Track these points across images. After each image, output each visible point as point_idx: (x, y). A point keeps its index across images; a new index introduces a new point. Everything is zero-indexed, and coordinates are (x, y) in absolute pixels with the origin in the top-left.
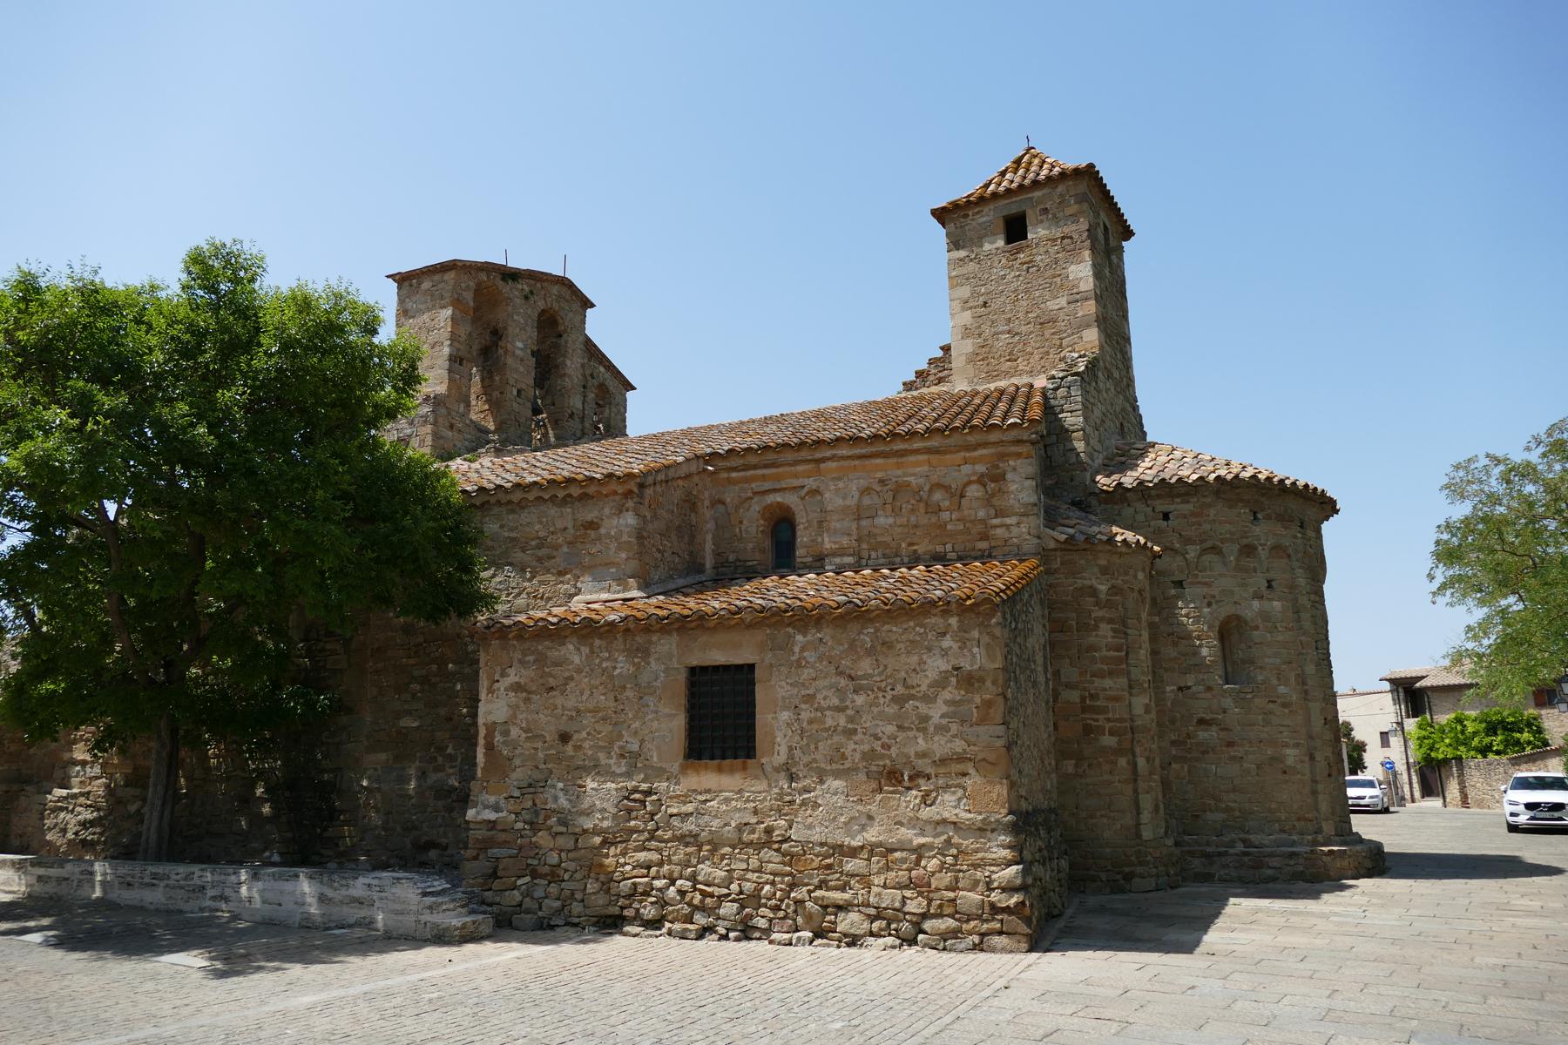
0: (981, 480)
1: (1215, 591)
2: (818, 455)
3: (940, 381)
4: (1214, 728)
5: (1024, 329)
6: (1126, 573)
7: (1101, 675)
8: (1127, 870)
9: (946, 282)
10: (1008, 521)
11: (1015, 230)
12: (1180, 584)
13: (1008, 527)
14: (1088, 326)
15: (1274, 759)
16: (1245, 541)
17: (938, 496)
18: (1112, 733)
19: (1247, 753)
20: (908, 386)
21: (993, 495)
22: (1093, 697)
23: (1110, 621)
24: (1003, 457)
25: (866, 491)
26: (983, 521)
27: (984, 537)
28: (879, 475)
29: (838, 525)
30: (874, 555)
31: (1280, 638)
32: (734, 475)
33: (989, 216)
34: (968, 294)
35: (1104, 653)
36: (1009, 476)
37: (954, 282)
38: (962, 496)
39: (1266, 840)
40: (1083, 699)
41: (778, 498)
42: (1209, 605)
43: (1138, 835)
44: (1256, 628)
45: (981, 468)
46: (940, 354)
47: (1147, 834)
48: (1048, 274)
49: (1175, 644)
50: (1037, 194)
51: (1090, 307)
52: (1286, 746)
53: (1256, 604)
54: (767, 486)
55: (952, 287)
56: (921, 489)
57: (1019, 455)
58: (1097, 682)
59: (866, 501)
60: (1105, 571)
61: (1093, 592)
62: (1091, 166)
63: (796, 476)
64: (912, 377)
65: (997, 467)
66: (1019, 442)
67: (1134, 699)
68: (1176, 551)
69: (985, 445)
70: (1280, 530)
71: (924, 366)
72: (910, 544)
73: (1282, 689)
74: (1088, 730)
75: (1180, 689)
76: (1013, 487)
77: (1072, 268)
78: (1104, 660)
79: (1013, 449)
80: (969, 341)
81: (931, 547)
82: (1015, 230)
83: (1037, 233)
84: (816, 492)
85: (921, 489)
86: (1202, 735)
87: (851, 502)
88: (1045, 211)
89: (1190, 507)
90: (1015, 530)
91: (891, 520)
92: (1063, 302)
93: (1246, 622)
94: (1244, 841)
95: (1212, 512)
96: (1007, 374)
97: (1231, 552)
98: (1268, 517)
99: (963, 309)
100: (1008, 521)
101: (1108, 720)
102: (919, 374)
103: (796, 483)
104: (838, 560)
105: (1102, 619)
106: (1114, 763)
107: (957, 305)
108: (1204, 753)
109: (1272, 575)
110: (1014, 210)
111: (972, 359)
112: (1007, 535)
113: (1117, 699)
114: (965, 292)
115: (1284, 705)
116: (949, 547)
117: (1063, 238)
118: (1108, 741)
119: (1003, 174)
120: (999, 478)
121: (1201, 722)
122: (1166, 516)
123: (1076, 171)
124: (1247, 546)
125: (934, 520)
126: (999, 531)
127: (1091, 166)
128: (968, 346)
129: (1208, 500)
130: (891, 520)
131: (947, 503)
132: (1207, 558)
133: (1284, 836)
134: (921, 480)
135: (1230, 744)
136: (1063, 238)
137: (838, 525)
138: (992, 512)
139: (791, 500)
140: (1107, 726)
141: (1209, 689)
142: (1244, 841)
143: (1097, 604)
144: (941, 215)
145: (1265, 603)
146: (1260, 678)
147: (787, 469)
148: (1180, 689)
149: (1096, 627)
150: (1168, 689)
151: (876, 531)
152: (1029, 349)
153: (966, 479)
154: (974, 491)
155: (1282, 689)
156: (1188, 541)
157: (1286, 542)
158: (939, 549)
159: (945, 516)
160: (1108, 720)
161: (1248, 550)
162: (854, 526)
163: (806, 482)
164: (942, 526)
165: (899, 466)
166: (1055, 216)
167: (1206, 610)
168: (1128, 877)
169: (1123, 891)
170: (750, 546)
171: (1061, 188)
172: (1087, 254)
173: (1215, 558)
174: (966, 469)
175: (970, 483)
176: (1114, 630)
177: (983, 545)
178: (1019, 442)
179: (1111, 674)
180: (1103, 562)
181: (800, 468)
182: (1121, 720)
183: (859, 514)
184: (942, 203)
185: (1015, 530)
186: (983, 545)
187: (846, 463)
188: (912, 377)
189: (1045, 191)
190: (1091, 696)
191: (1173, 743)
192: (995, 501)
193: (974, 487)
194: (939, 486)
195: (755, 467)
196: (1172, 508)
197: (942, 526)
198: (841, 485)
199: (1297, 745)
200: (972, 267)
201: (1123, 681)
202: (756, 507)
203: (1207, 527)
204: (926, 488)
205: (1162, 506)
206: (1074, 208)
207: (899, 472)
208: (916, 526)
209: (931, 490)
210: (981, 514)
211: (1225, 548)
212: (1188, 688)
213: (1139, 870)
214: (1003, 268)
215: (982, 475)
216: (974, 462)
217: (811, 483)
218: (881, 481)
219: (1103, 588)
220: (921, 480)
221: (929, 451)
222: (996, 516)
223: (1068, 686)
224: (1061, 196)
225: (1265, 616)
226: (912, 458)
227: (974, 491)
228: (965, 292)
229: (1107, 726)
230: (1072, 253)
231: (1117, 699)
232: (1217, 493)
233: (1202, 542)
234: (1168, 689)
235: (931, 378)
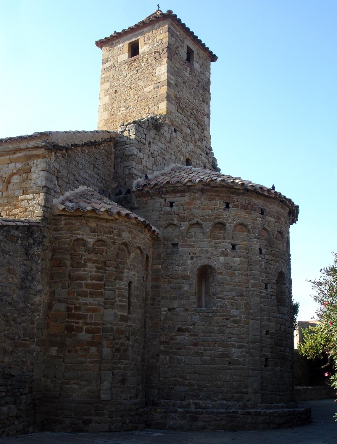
0: (18, 172)
1: (197, 250)
4: (187, 334)
6: (110, 233)
7: (84, 294)
8: (86, 418)
12: (175, 245)
14: (162, 101)
15: (224, 355)
16: (217, 220)
18: (87, 331)
19: (205, 350)
21: (23, 181)
22: (77, 308)
23: (95, 262)
24: (30, 158)
31: (237, 279)
33: (124, 46)
34: (109, 87)
35: (89, 282)
36: (32, 170)
37: (104, 80)
38: (9, 182)
39: (210, 403)
40: (69, 309)
42: (192, 258)
43: (99, 397)
44: (221, 274)
45: (19, 165)
47: (103, 397)
49: (169, 282)
51: (164, 90)
52: (234, 346)
53: (222, 259)
57: (38, 156)
58: (82, 300)
60: (93, 230)
61: (84, 243)
62: (170, 12)
65: (28, 164)
66: (37, 148)
67: (105, 310)
68: (175, 225)
69: (20, 150)
70: (243, 214)
73: (234, 311)
74: (70, 328)
75: (170, 310)
78: (87, 286)
79: (35, 152)
80: (106, 113)
86: (179, 338)
89: (186, 199)
90: (31, 203)
93: (214, 269)
94: (196, 404)
95: (198, 202)
97: (208, 226)
98: (236, 207)
101: (86, 324)
105: (89, 260)
106: (87, 350)
108: (179, 349)
109: (235, 242)
110: (134, 40)
112: (27, 205)
113: (95, 311)
114: (107, 85)
115: (234, 322)
117: (155, 52)
118: (84, 336)
120: (28, 171)
121: (180, 330)
122: (172, 205)
124: (220, 223)
126: (23, 202)
129: (197, 195)
132: (193, 230)
133: (224, 402)
135: (195, 345)
140: (85, 327)
141: (186, 310)
142: (196, 404)
143: (87, 250)
144: (101, 44)
145: (229, 258)
146: (220, 304)
148: (170, 310)
149: (85, 265)
150: (163, 309)
153: (11, 172)
155: (234, 311)
156: (182, 219)
157: (248, 222)
160: (86, 324)
161: (221, 225)
167: (190, 262)
168: (87, 422)
169: (82, 431)
172: (165, 60)
173: (199, 230)
174: (12, 166)
175: (13, 174)
176: (98, 268)
178: (37, 148)
179: (92, 294)
180: (93, 224)
182: (96, 324)
185: (31, 203)
190: (76, 307)
191: (162, 343)
192: (24, 185)
193: (15, 177)
196: (175, 199)
199: (241, 347)
201: (101, 300)
203: (194, 211)
211: (204, 224)
212: (174, 309)
213: (97, 418)
216: (15, 161)
219: (91, 241)
223: (60, 301)
225: (228, 267)
227: (16, 179)
229: (85, 327)
230: (158, 61)
231: (95, 311)
232: (202, 190)
233: (190, 220)
234: (163, 309)
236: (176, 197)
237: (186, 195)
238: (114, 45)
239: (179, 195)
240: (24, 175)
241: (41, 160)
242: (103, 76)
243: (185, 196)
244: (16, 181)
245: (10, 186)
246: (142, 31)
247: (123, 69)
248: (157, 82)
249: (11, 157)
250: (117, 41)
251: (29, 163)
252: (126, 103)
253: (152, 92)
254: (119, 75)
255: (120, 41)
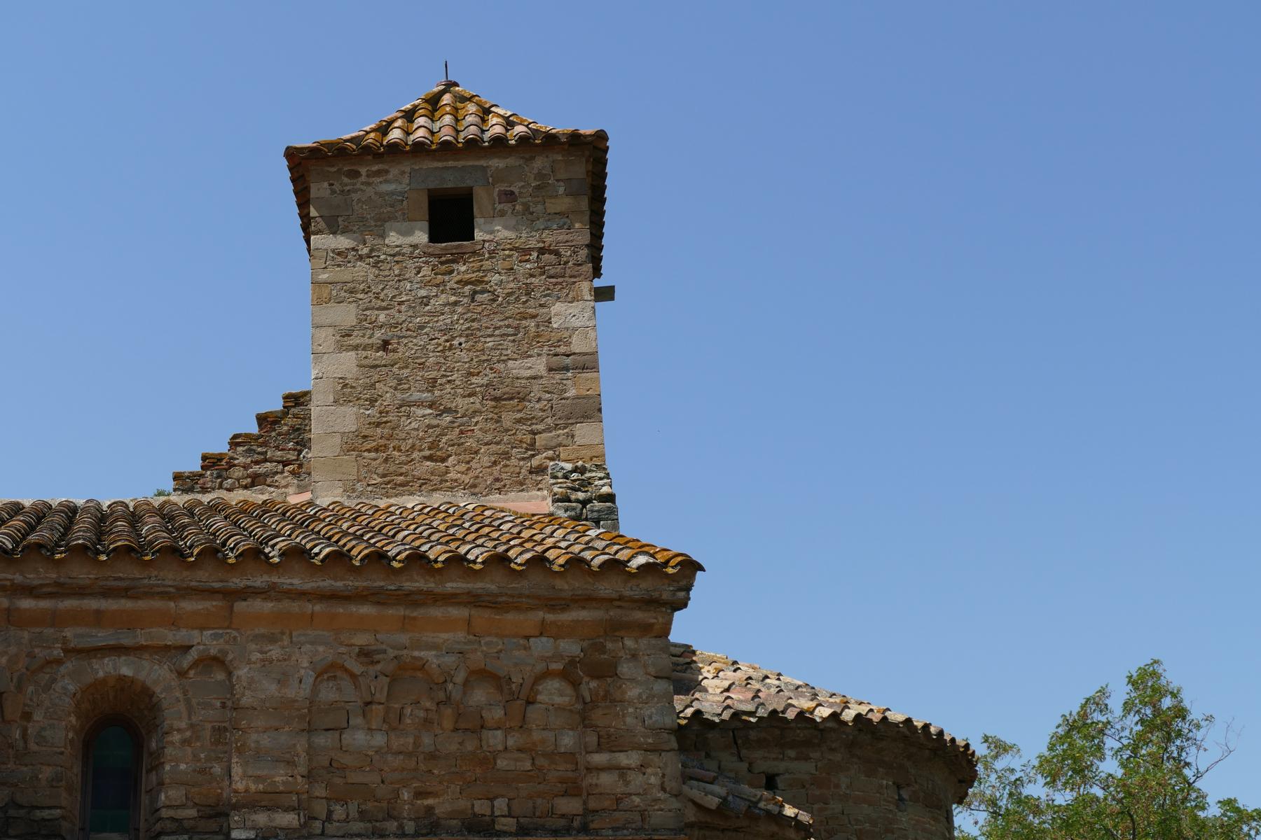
2: (237, 582)
3: (255, 481)
5: (462, 403)
9: (306, 292)
10: (624, 759)
11: (450, 219)
13: (622, 771)
17: (479, 696)
20: (184, 482)
24: (615, 629)
25: (329, 671)
26: (570, 756)
27: (572, 789)
28: (361, 640)
29: (265, 741)
30: (339, 812)
32: (26, 604)
36: (625, 669)
37: (324, 293)
41: (105, 668)
45: (571, 647)
46: (254, 429)
48: (512, 310)
50: (496, 163)
54: (103, 637)
55: (319, 301)
56: (448, 677)
59: (328, 694)
62: (601, 137)
63: (174, 622)
64: (196, 466)
65: (602, 649)
71: (224, 448)
72: (419, 794)
76: (633, 692)
77: (558, 307)
79: (639, 615)
81: (463, 804)
82: (450, 219)
83: (490, 232)
84: (218, 661)
85: (448, 677)
87: (298, 692)
88: (509, 197)
90: (637, 780)
91: (379, 740)
92: (539, 365)
95: (844, 781)
96: (424, 484)
99: (341, 348)
100: (624, 759)
102: (210, 461)
103: (171, 637)
104: (261, 818)
107: (328, 338)
110: (450, 182)
111: (354, 444)
112: (620, 789)
114: (347, 315)
116: (501, 805)
117: (542, 251)
119: (409, 115)
120: (605, 671)
123: (575, 137)
125: (470, 746)
126: (606, 779)
127: (601, 137)
128: (349, 418)
129: (837, 757)
130: (379, 740)
131: (498, 713)
134: (450, 660)
136: (542, 251)
137: (265, 741)
138: (592, 739)
139: (155, 674)
147: (158, 604)
151: (347, 760)
152: (470, 443)
153: (540, 667)
154: (554, 693)
158: (481, 807)
159: (495, 739)
162: (301, 745)
163: (195, 636)
164: (487, 761)
165: (405, 624)
166: (527, 209)
170: (46, 773)
171: (539, 163)
174: (542, 646)
177: (570, 806)
181: (188, 606)
183: (311, 719)
184: (305, 141)
185: (637, 780)
186: (570, 806)
187: (295, 607)
188: (196, 466)
189: (511, 161)
194: (483, 675)
195: (81, 592)
196: (781, 766)
197: (487, 761)
198: (275, 652)
200: (361, 270)
202: (68, 683)
204: (460, 677)
205: (766, 762)
206: (564, 203)
207: (403, 638)
208: (432, 756)
209: (466, 683)
210: (568, 741)
214: (425, 284)
215: (572, 662)
216: (557, 632)
217: (206, 641)
218: (366, 654)
220: (450, 660)
221: (474, 600)
222: (600, 748)
224: (540, 176)
226: (437, 612)
228: (347, 315)
235: (237, 472)
236: (782, 760)
237: (811, 755)
238: (363, 179)
239: (792, 753)
240: (593, 684)
241: (653, 641)
242: (324, 277)
243: (807, 759)
244: (558, 700)
245: (533, 713)
246: (483, 163)
247: (410, 273)
248: (562, 349)
249: (550, 617)
250: (375, 168)
251: (609, 645)
252: (437, 393)
253: (543, 381)
254: (390, 293)
255: (387, 172)
